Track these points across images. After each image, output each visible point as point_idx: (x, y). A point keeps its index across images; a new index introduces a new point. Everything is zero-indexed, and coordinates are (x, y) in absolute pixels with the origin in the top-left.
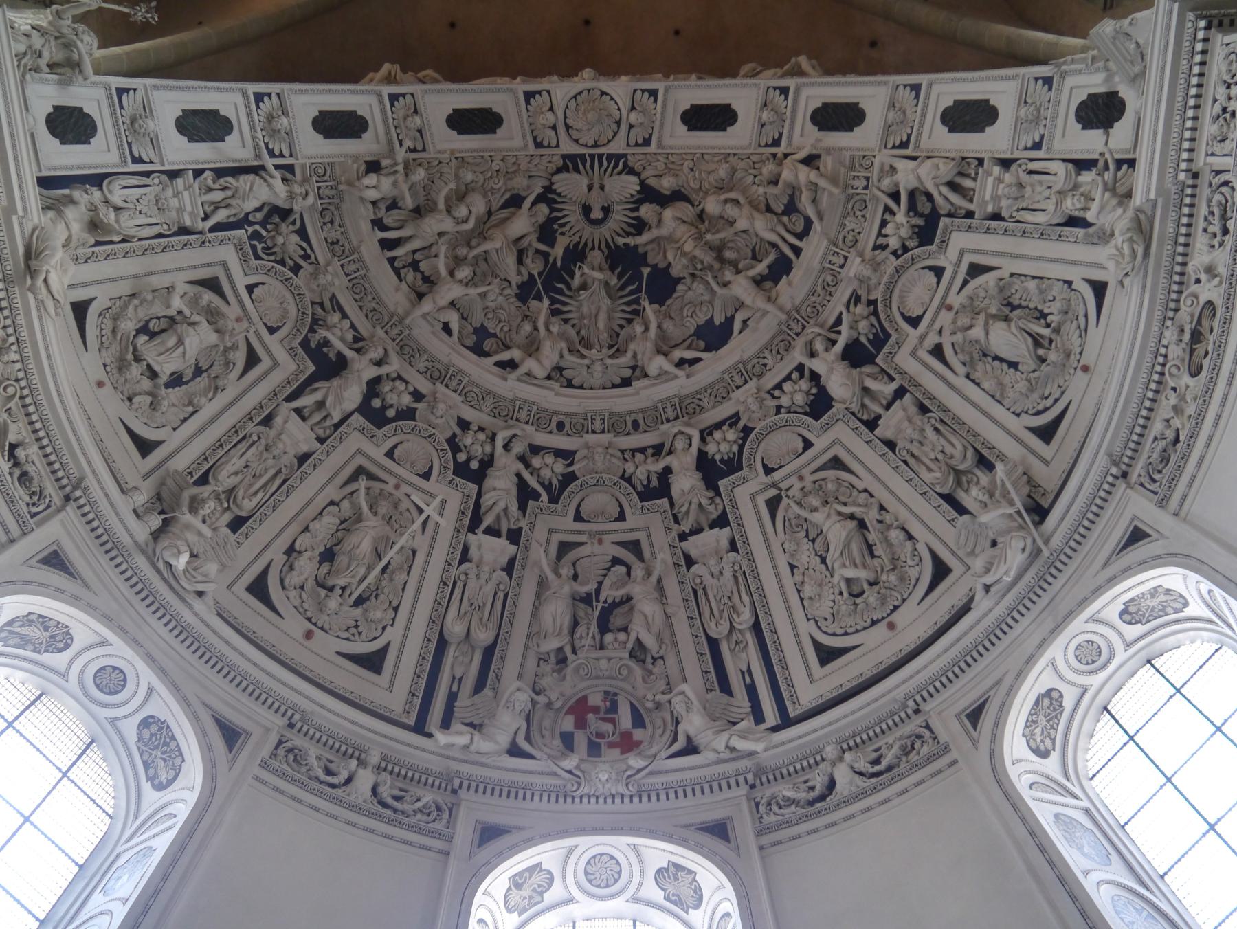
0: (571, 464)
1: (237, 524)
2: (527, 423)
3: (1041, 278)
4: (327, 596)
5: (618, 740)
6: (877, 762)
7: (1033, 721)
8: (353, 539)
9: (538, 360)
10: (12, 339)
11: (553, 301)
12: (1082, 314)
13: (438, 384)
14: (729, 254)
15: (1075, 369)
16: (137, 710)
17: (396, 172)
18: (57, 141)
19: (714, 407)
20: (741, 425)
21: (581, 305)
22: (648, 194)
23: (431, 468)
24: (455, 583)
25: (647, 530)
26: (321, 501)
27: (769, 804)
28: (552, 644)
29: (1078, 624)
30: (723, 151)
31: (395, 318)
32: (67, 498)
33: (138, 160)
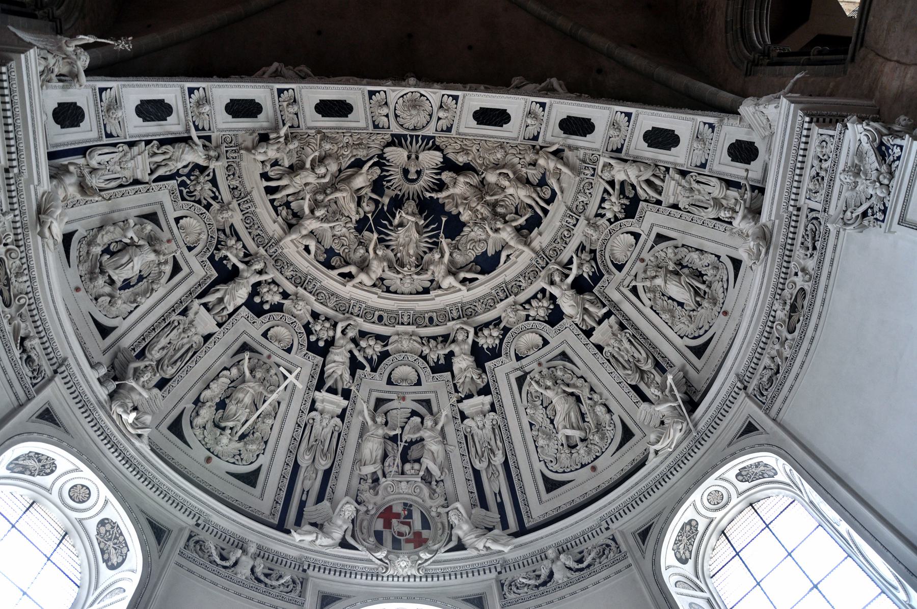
0: (386, 345)
1: (162, 384)
2: (358, 316)
3: (701, 251)
4: (221, 434)
5: (412, 537)
6: (580, 561)
7: (680, 541)
8: (241, 396)
9: (368, 274)
10: (25, 266)
11: (380, 233)
12: (725, 279)
13: (299, 288)
14: (500, 210)
15: (719, 313)
16: (97, 514)
17: (279, 142)
18: (59, 126)
19: (484, 312)
20: (502, 326)
21: (399, 237)
22: (448, 165)
23: (292, 345)
24: (306, 425)
25: (436, 393)
26: (217, 367)
27: (510, 585)
28: (368, 470)
29: (711, 481)
30: (499, 140)
31: (273, 241)
32: (55, 372)
33: (109, 136)
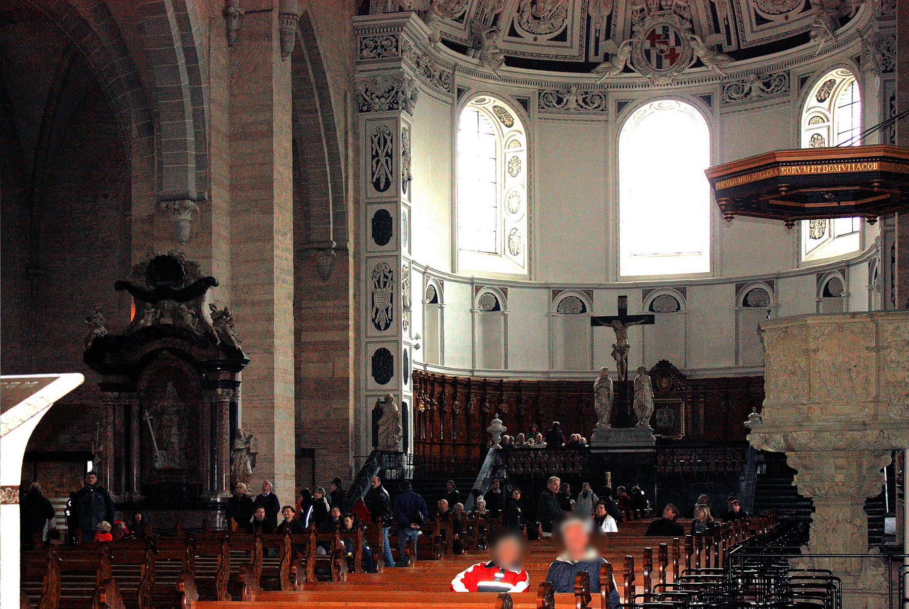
6: (768, 85)
28: (638, 8)
